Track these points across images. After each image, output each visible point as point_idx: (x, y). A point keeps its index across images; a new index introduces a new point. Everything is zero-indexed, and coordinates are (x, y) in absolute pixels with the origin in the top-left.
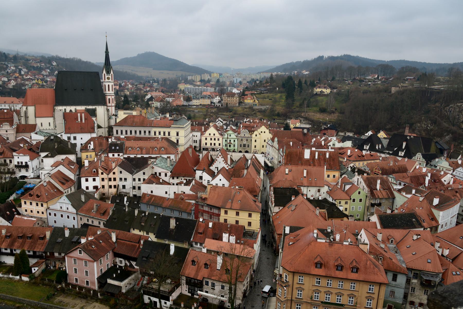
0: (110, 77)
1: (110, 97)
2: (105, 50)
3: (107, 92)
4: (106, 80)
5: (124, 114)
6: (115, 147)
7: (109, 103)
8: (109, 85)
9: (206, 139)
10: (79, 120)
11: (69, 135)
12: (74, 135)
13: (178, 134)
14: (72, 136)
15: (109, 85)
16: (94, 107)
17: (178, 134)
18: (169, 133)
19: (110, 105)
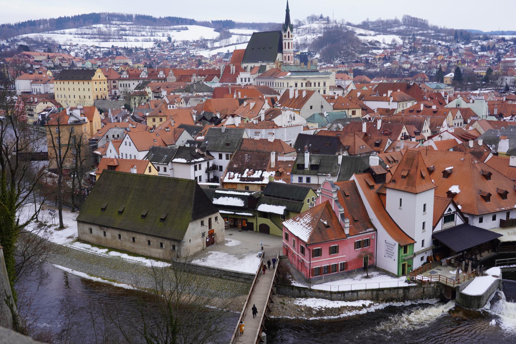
0: (287, 34)
2: (286, 8)
3: (284, 50)
7: (289, 60)
8: (289, 43)
15: (289, 43)
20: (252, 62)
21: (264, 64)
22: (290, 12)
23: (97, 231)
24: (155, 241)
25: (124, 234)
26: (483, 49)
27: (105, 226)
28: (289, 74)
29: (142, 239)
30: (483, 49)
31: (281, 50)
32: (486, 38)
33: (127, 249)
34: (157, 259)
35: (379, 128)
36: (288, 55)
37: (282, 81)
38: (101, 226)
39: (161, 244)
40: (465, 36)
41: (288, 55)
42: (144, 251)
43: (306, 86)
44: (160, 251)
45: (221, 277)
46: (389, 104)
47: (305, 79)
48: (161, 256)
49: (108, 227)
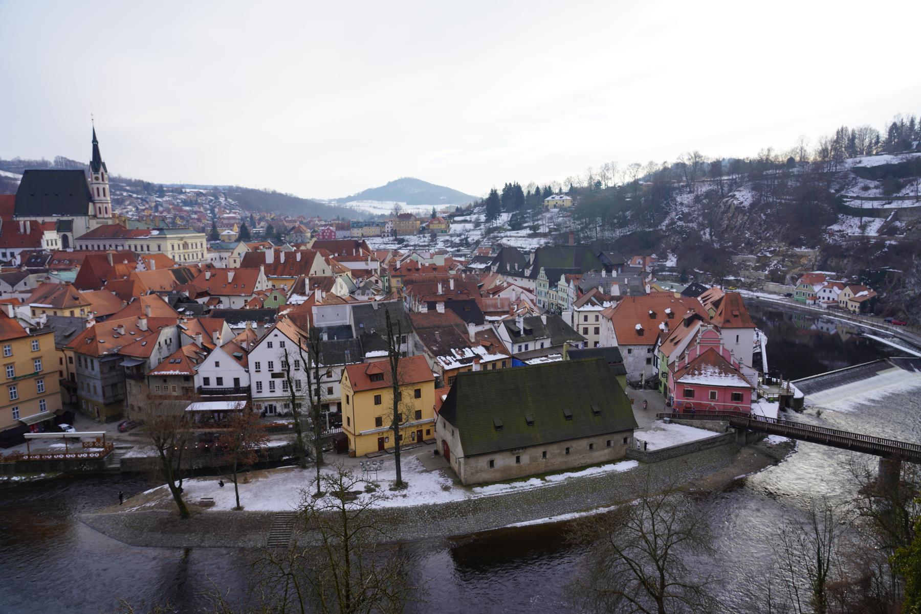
0: (100, 176)
1: (100, 205)
2: (91, 139)
3: (96, 198)
4: (94, 181)
5: (97, 223)
6: (36, 259)
9: (235, 261)
10: (22, 230)
11: (4, 251)
12: (12, 250)
13: (159, 246)
14: (8, 251)
16: (70, 218)
17: (159, 246)
18: (148, 247)
19: (101, 216)
20: (38, 215)
21: (65, 218)
22: (100, 146)
23: (503, 461)
24: (599, 441)
25: (553, 449)
26: (185, 203)
27: (519, 449)
28: (155, 233)
29: (584, 443)
30: (185, 203)
31: (90, 198)
32: (178, 190)
33: (556, 467)
34: (599, 465)
35: (452, 288)
36: (105, 205)
37: (145, 243)
38: (512, 450)
39: (609, 443)
40: (146, 187)
41: (105, 205)
42: (583, 461)
43: (184, 248)
44: (606, 451)
45: (700, 450)
46: (367, 264)
47: (182, 239)
48: (602, 459)
49: (525, 448)
